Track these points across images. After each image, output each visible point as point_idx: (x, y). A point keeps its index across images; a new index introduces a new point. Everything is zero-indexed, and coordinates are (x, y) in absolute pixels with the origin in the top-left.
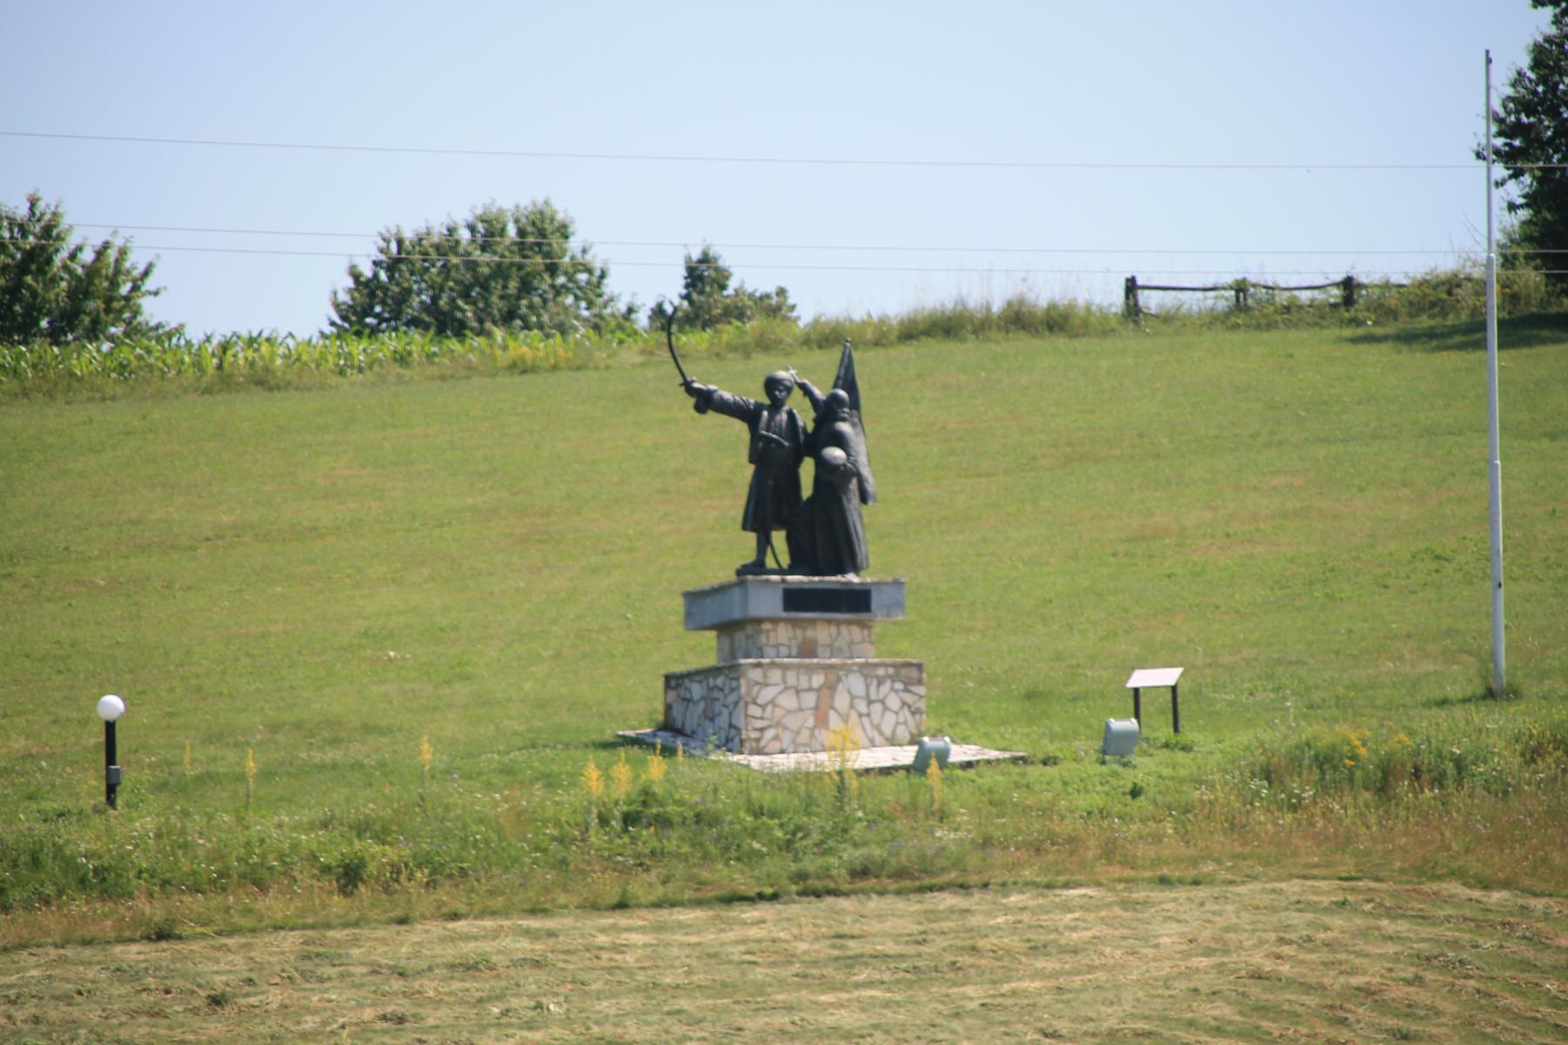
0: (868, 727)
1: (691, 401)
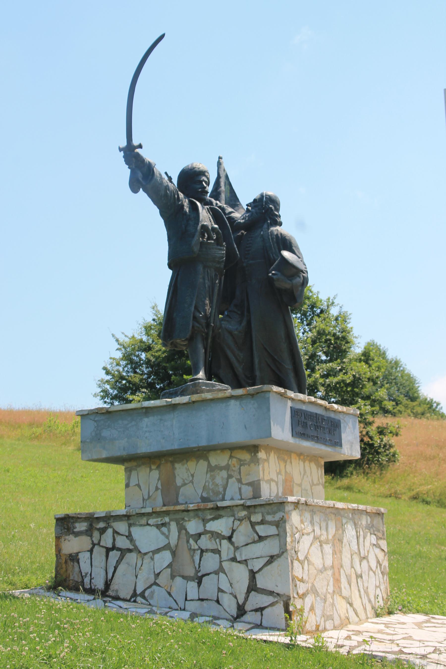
1: (126, 172)
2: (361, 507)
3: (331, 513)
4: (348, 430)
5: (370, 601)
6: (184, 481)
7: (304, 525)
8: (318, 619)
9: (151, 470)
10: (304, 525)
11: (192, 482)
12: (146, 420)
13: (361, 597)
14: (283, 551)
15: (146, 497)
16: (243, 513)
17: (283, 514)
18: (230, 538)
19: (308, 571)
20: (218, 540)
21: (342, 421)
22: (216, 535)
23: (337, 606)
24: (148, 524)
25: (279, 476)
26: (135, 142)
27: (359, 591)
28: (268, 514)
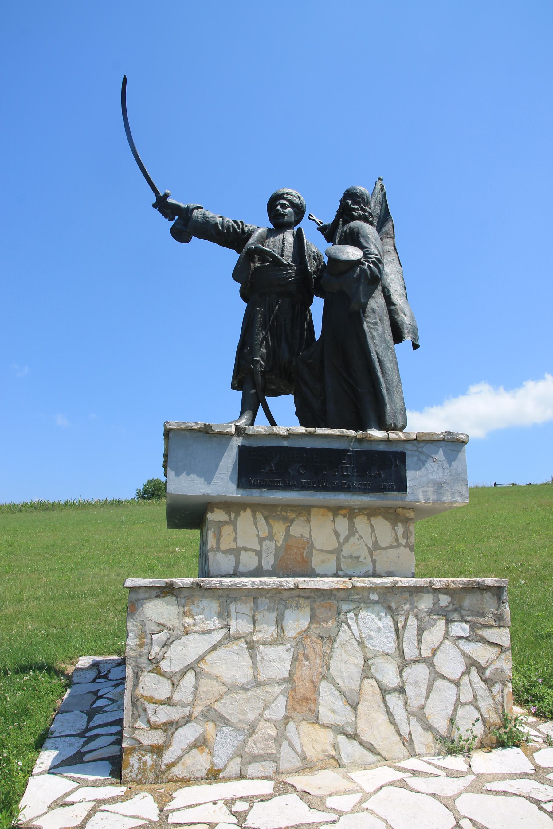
0: (400, 714)
3: (299, 596)
4: (430, 464)
5: (429, 728)
7: (195, 619)
10: (195, 619)
13: (393, 722)
19: (196, 688)
21: (408, 453)
27: (389, 714)
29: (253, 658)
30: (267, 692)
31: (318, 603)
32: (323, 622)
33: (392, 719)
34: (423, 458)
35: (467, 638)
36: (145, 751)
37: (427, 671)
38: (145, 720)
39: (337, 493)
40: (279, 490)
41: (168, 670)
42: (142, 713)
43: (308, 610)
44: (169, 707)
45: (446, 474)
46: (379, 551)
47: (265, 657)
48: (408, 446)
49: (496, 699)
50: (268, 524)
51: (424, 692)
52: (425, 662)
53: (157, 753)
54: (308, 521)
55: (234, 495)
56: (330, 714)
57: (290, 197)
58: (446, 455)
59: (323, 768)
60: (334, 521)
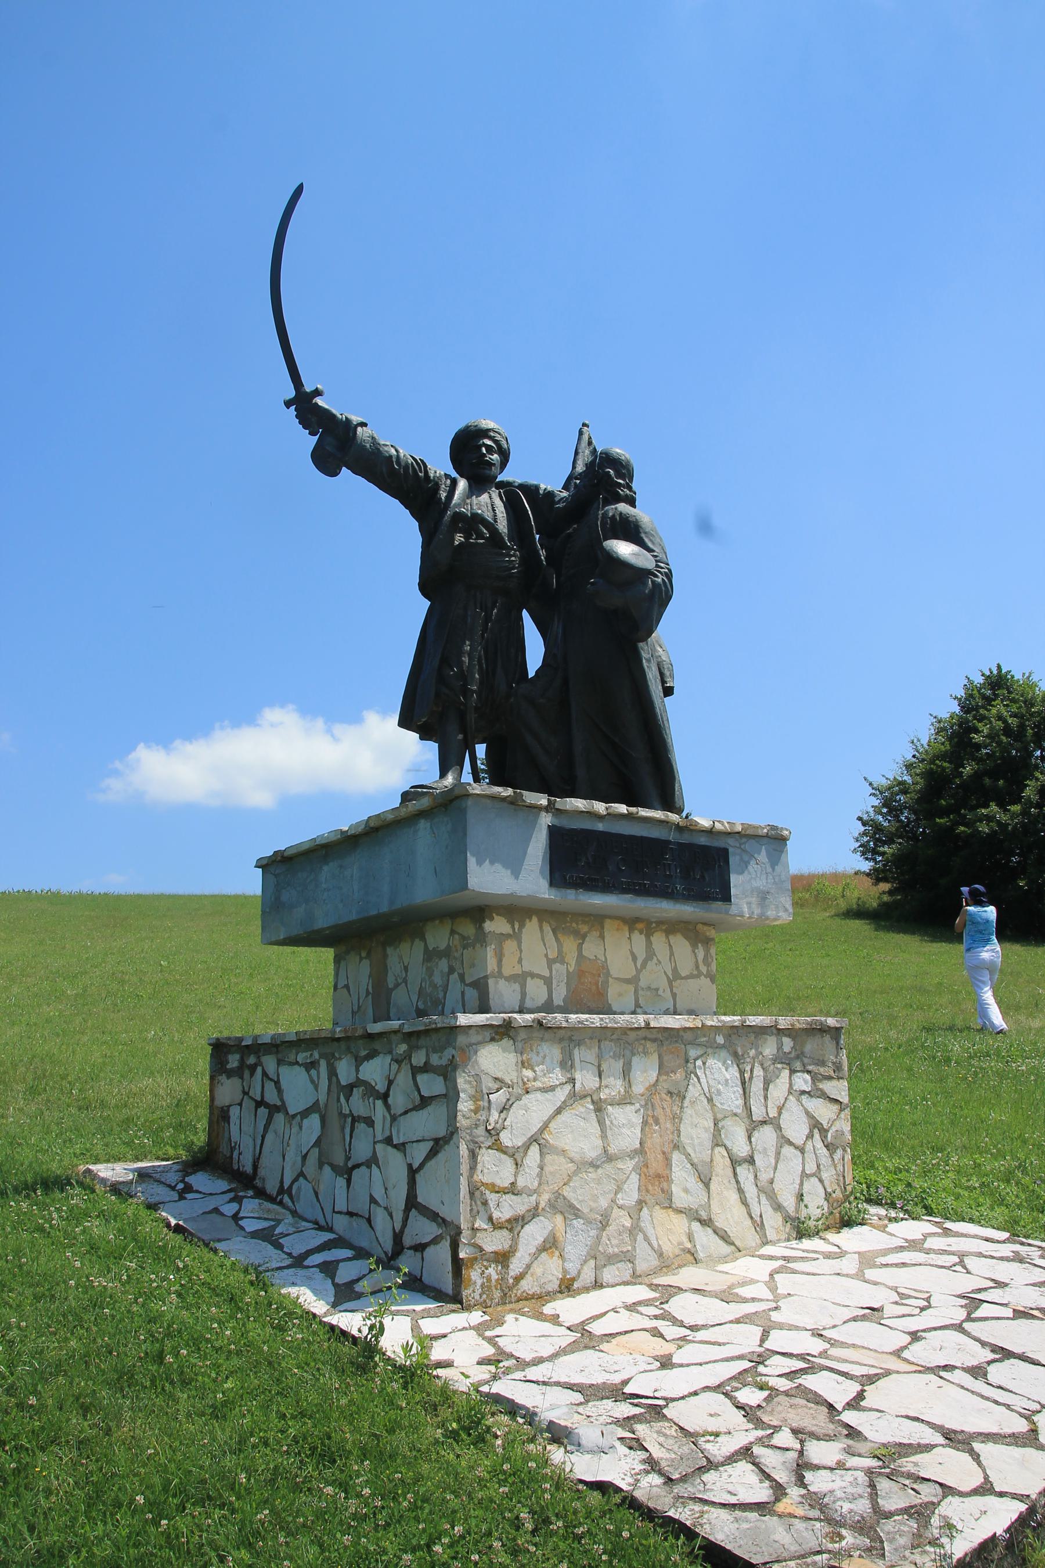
0: (751, 1191)
2: (753, 1020)
3: (645, 1038)
4: (753, 866)
5: (778, 1207)
6: (396, 980)
7: (535, 1071)
8: (569, 1266)
9: (361, 959)
10: (535, 1071)
11: (405, 981)
12: (326, 868)
13: (744, 1202)
14: (453, 1132)
15: (356, 1008)
16: (403, 1048)
17: (454, 1052)
18: (385, 1097)
19: (541, 1168)
20: (371, 1099)
21: (731, 850)
22: (370, 1091)
23: (651, 1233)
24: (297, 1063)
25: (556, 966)
26: (308, 388)
27: (740, 1191)
28: (435, 1051)
29: (601, 1123)
30: (619, 1169)
31: (665, 1048)
32: (672, 1072)
33: (743, 1198)
34: (746, 858)
35: (808, 1093)
36: (488, 1260)
37: (775, 1135)
38: (486, 1217)
39: (659, 900)
40: (596, 891)
41: (509, 1144)
42: (481, 1208)
43: (656, 1056)
44: (513, 1197)
45: (769, 881)
46: (679, 981)
47: (614, 1122)
48: (731, 841)
49: (838, 1169)
50: (557, 940)
51: (773, 1161)
52: (771, 1123)
53: (502, 1263)
54: (602, 937)
55: (547, 896)
56: (683, 1194)
57: (498, 438)
58: (769, 856)
59: (680, 1266)
60: (630, 938)
